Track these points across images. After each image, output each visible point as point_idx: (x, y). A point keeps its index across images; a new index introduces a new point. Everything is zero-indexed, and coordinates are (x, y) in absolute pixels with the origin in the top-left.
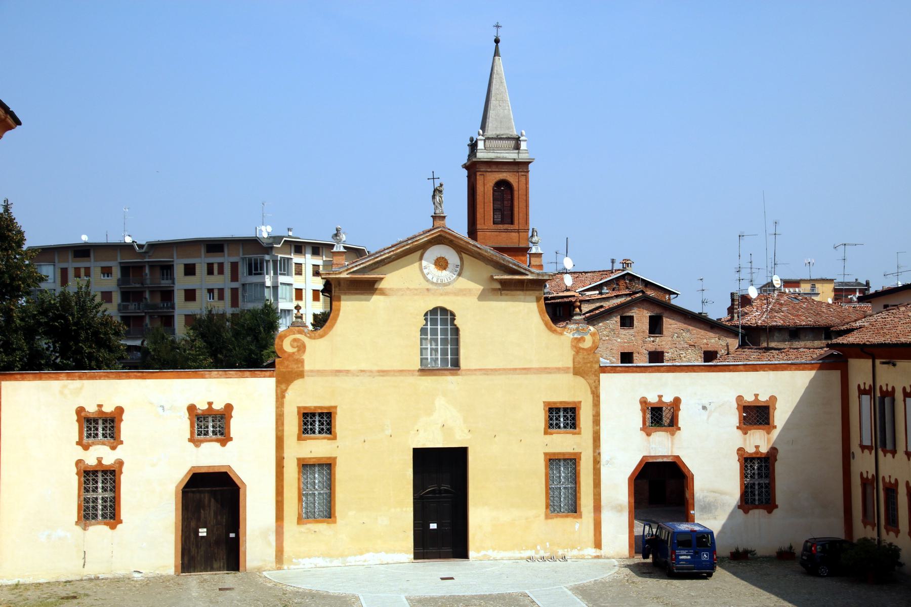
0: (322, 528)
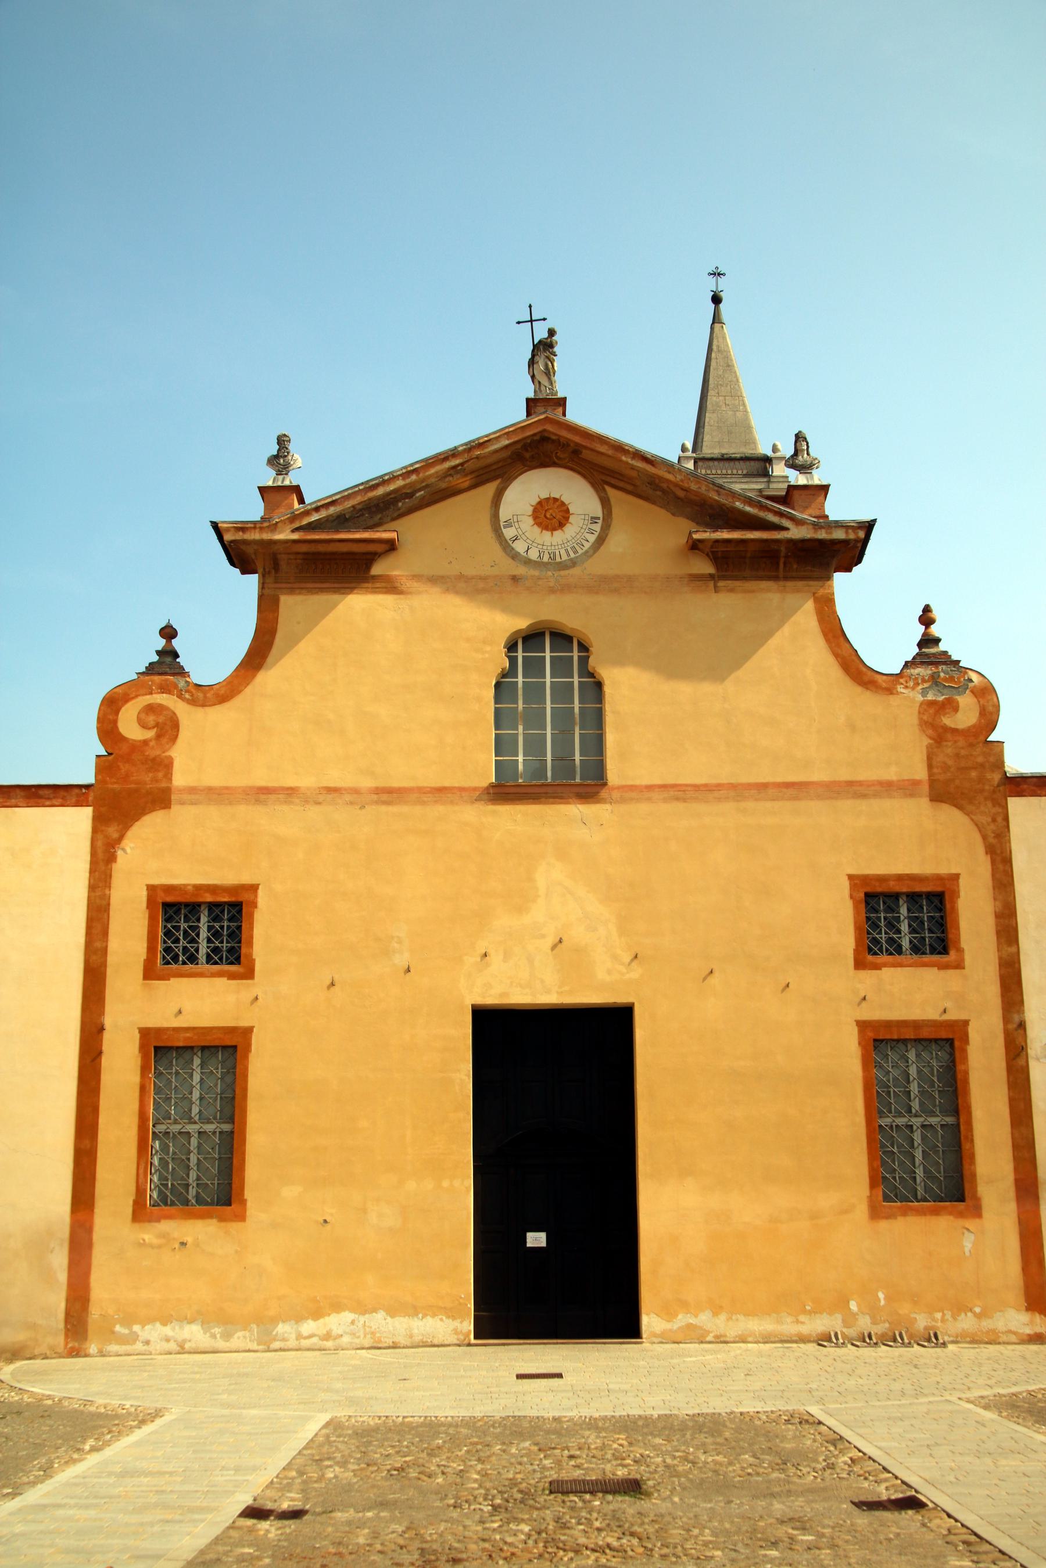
0: (201, 1231)
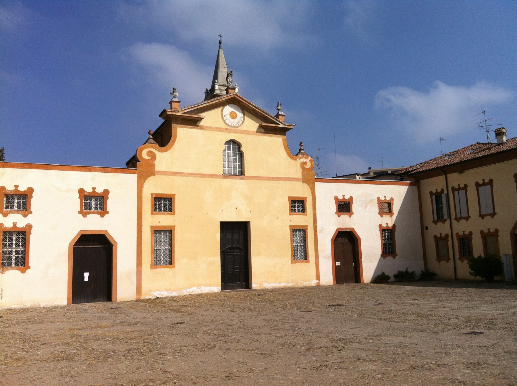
0: (166, 271)
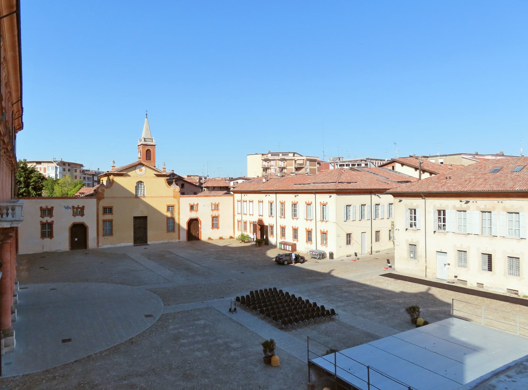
0: (109, 237)
